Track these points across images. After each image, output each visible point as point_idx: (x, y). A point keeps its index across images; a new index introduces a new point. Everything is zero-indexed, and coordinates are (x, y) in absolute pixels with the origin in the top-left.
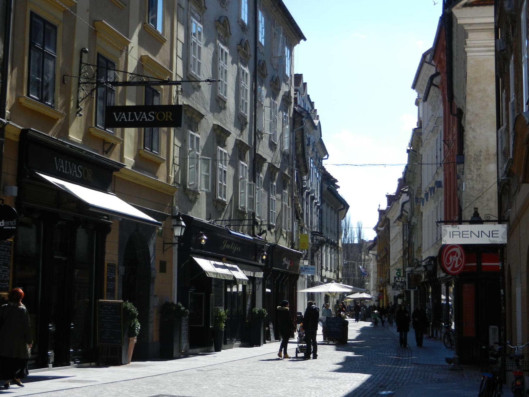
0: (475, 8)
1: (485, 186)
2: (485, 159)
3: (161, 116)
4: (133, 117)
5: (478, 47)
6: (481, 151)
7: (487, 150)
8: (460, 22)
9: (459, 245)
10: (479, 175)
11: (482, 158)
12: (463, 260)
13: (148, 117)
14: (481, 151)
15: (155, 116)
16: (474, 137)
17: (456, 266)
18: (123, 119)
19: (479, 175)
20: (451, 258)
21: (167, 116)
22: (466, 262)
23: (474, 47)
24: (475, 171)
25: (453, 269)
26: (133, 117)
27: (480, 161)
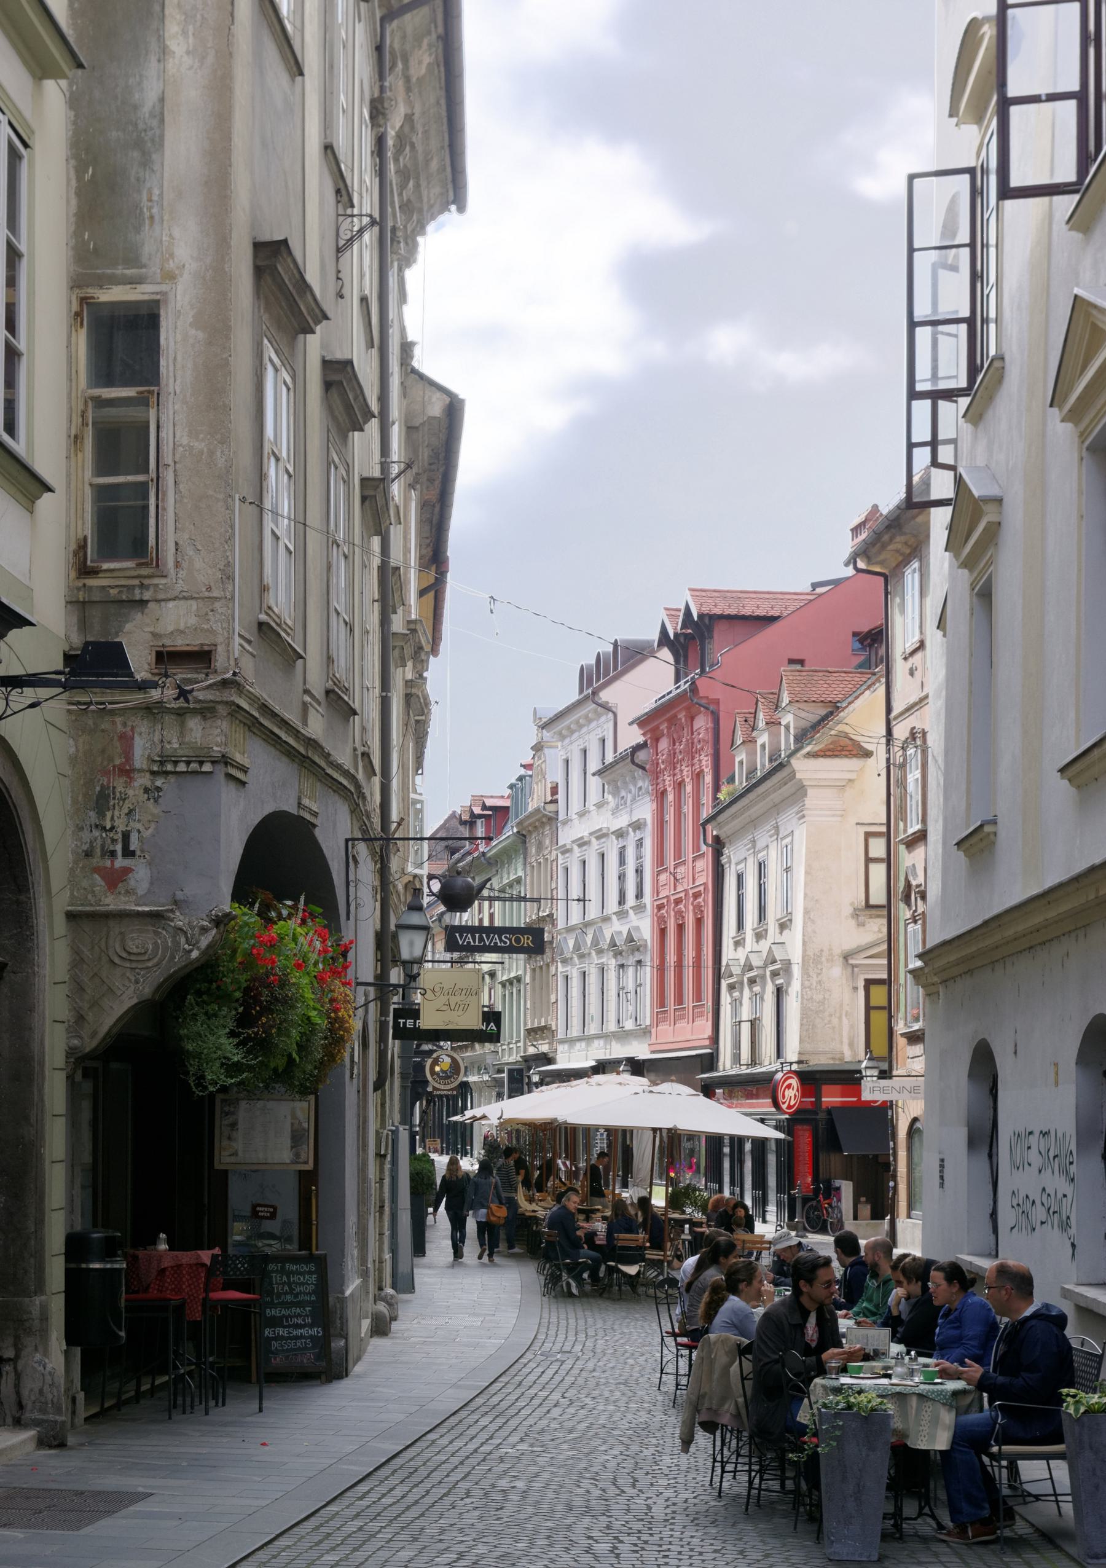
0: (821, 760)
1: (827, 996)
2: (828, 960)
3: (518, 940)
4: (481, 939)
5: (821, 809)
6: (822, 950)
7: (830, 950)
8: (798, 776)
9: (717, 1049)
10: (819, 982)
11: (823, 959)
12: (799, 1095)
13: (501, 940)
14: (822, 950)
15: (510, 940)
16: (814, 932)
17: (792, 1103)
18: (469, 943)
19: (819, 982)
20: (786, 1093)
21: (526, 941)
22: (803, 1096)
23: (816, 809)
24: (815, 976)
25: (789, 1107)
26: (481, 939)
27: (821, 963)
